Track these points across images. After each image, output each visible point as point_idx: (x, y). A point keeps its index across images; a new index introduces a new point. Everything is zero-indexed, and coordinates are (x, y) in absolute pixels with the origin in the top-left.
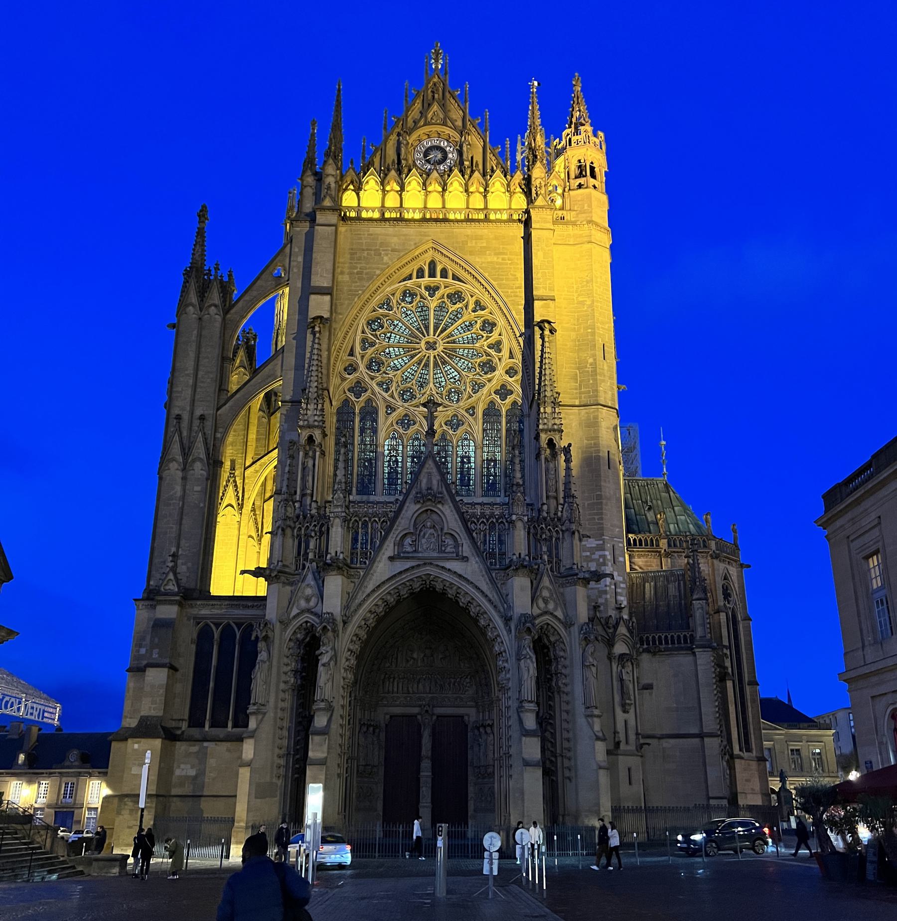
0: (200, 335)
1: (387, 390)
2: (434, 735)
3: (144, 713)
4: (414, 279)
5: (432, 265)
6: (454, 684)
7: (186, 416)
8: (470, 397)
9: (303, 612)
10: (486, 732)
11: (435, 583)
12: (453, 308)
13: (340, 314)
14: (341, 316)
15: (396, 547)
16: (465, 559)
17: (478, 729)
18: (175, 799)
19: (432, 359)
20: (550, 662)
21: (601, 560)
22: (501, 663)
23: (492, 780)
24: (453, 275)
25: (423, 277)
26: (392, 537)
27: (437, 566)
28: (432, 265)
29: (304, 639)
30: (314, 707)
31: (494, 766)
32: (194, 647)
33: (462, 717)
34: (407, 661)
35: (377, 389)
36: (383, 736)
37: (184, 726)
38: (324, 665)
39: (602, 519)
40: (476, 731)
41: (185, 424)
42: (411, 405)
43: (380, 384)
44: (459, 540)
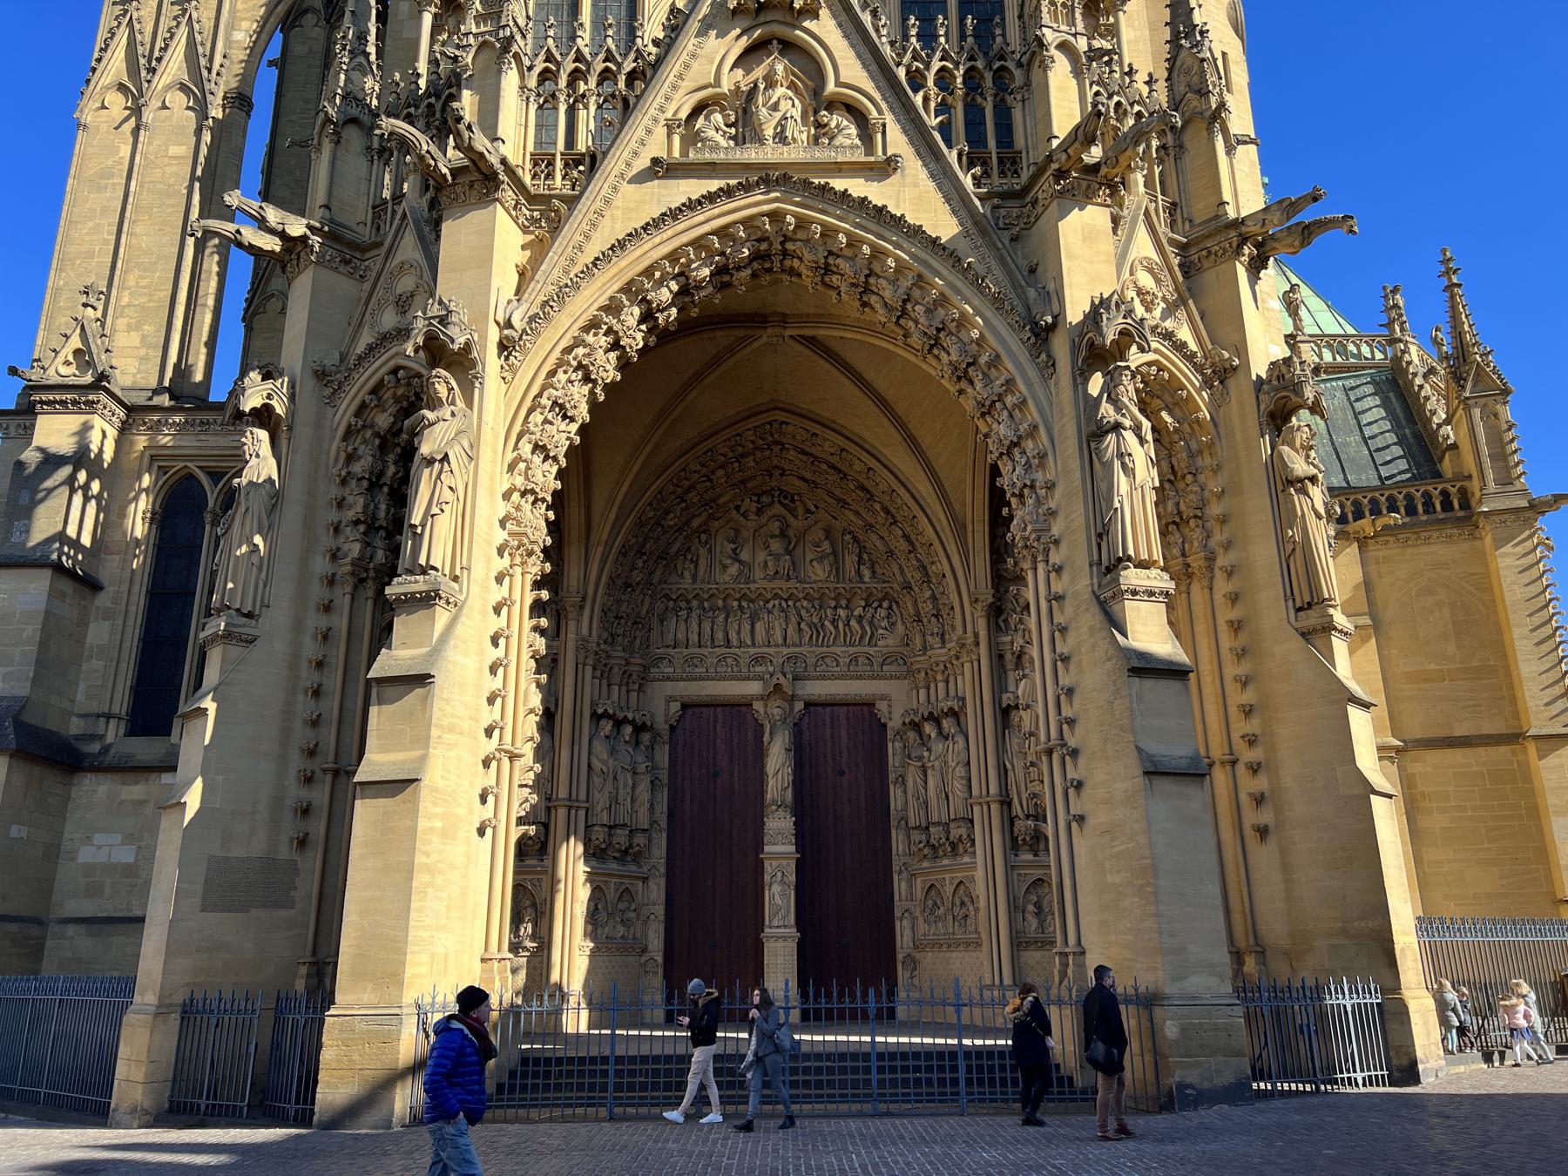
6: (847, 624)
17: (916, 727)
18: (71, 930)
23: (966, 859)
27: (807, 184)
30: (392, 590)
31: (972, 821)
34: (725, 567)
36: (663, 756)
37: (113, 733)
38: (430, 462)
40: (912, 735)
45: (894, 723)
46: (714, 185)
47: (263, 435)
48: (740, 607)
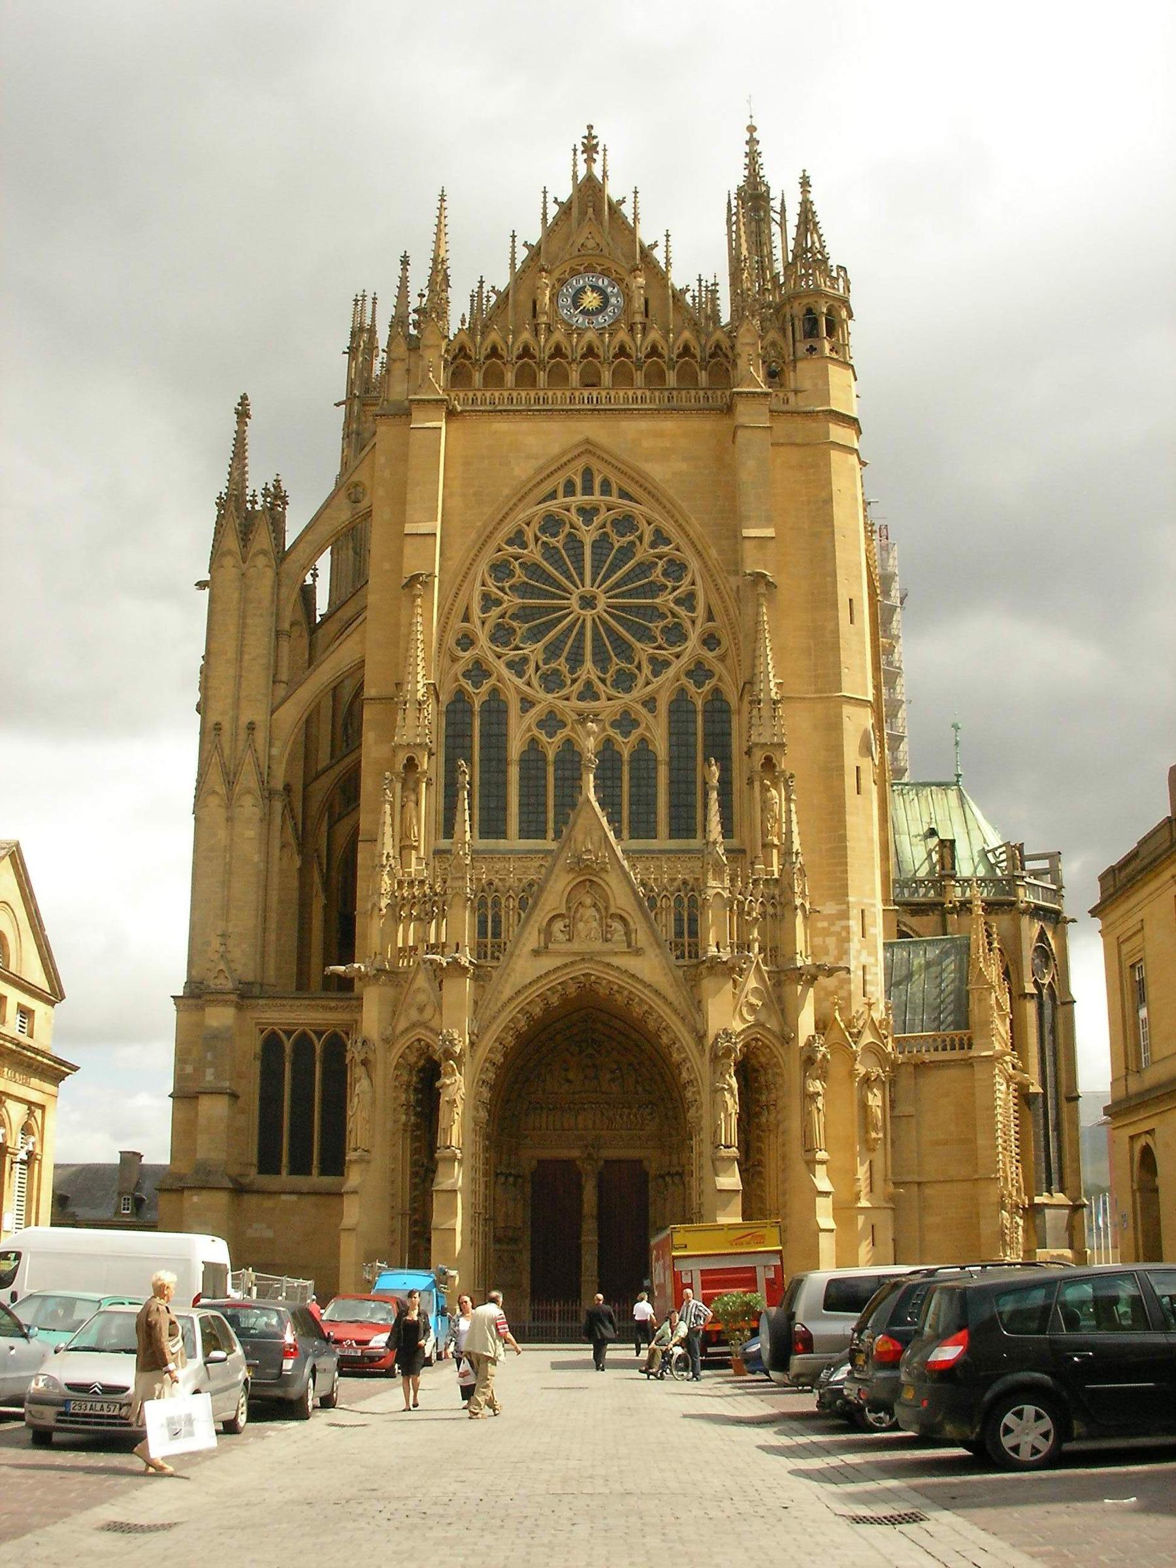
0: (244, 600)
1: (520, 674)
2: (600, 1187)
3: (201, 1155)
4: (561, 500)
5: (588, 474)
7: (227, 726)
8: (648, 684)
9: (414, 1025)
10: (673, 1182)
11: (598, 986)
12: (618, 542)
13: (449, 559)
14: (450, 563)
15: (542, 936)
16: (638, 952)
17: (663, 1177)
19: (589, 624)
20: (759, 1091)
21: (844, 934)
22: (690, 1094)
24: (620, 489)
25: (573, 494)
26: (536, 922)
28: (588, 474)
29: (416, 1063)
30: (436, 1155)
32: (258, 1063)
33: (640, 1162)
35: (506, 673)
36: (528, 1189)
37: (253, 1171)
39: (846, 872)
40: (660, 1181)
41: (226, 738)
42: (558, 698)
43: (510, 665)
44: (632, 924)
45: (652, 1172)
46: (558, 962)
47: (363, 1069)
48: (569, 1108)
